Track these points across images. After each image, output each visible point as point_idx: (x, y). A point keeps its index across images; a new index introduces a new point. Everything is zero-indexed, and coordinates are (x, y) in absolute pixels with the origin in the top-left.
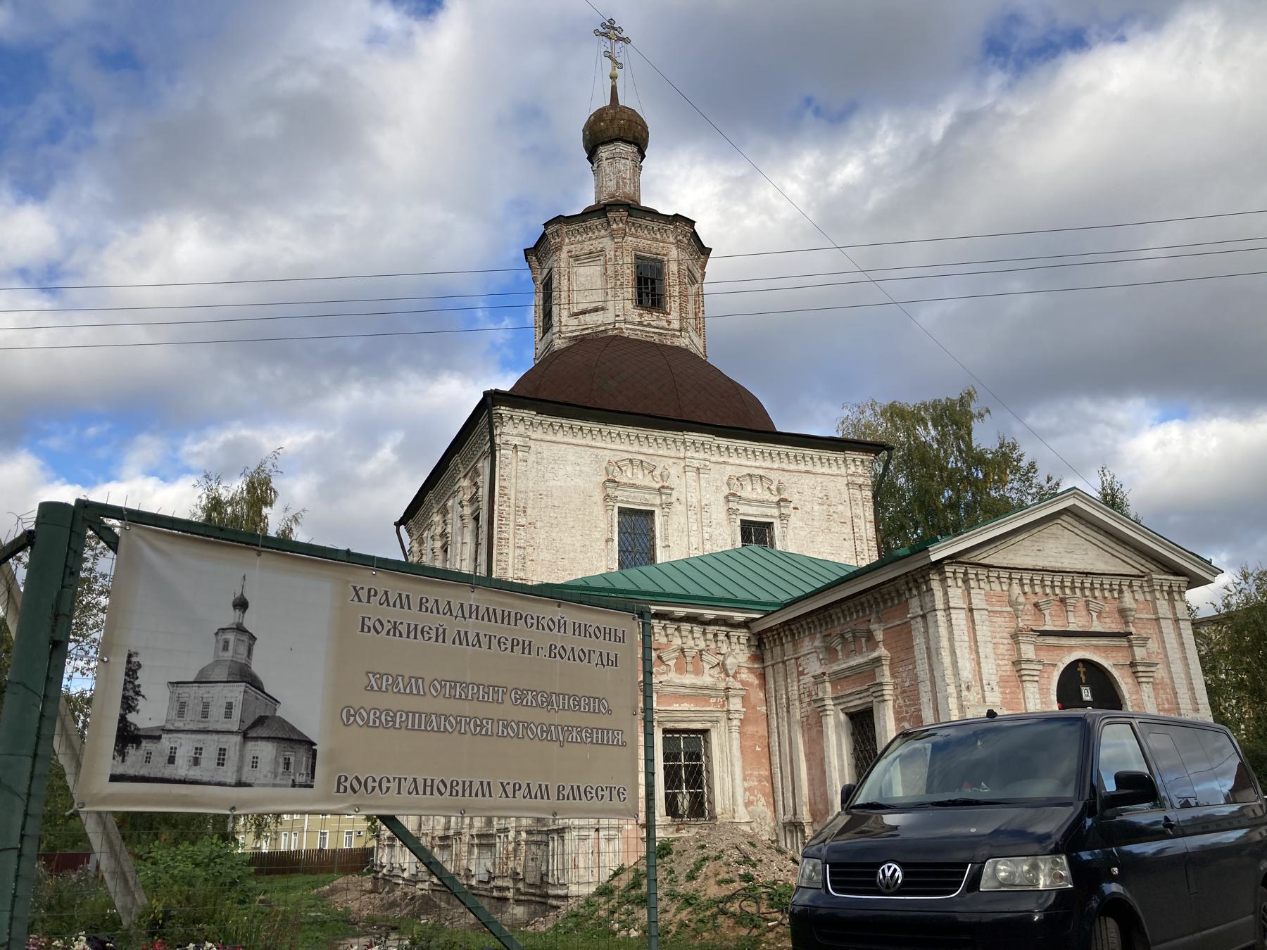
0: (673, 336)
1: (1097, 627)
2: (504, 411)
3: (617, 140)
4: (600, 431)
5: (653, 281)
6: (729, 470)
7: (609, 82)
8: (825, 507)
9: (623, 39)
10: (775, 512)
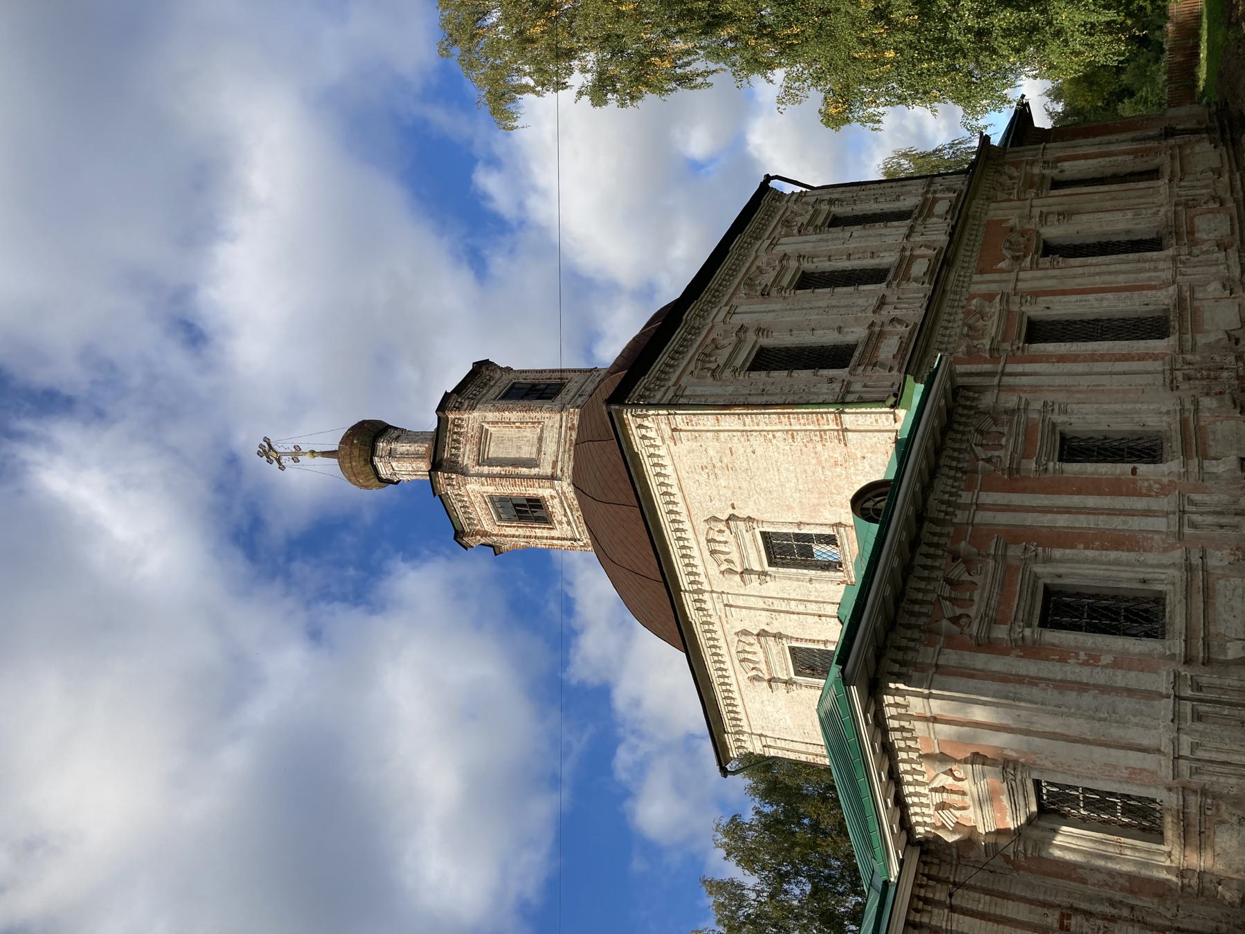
5: (515, 505)
7: (319, 459)
9: (269, 445)
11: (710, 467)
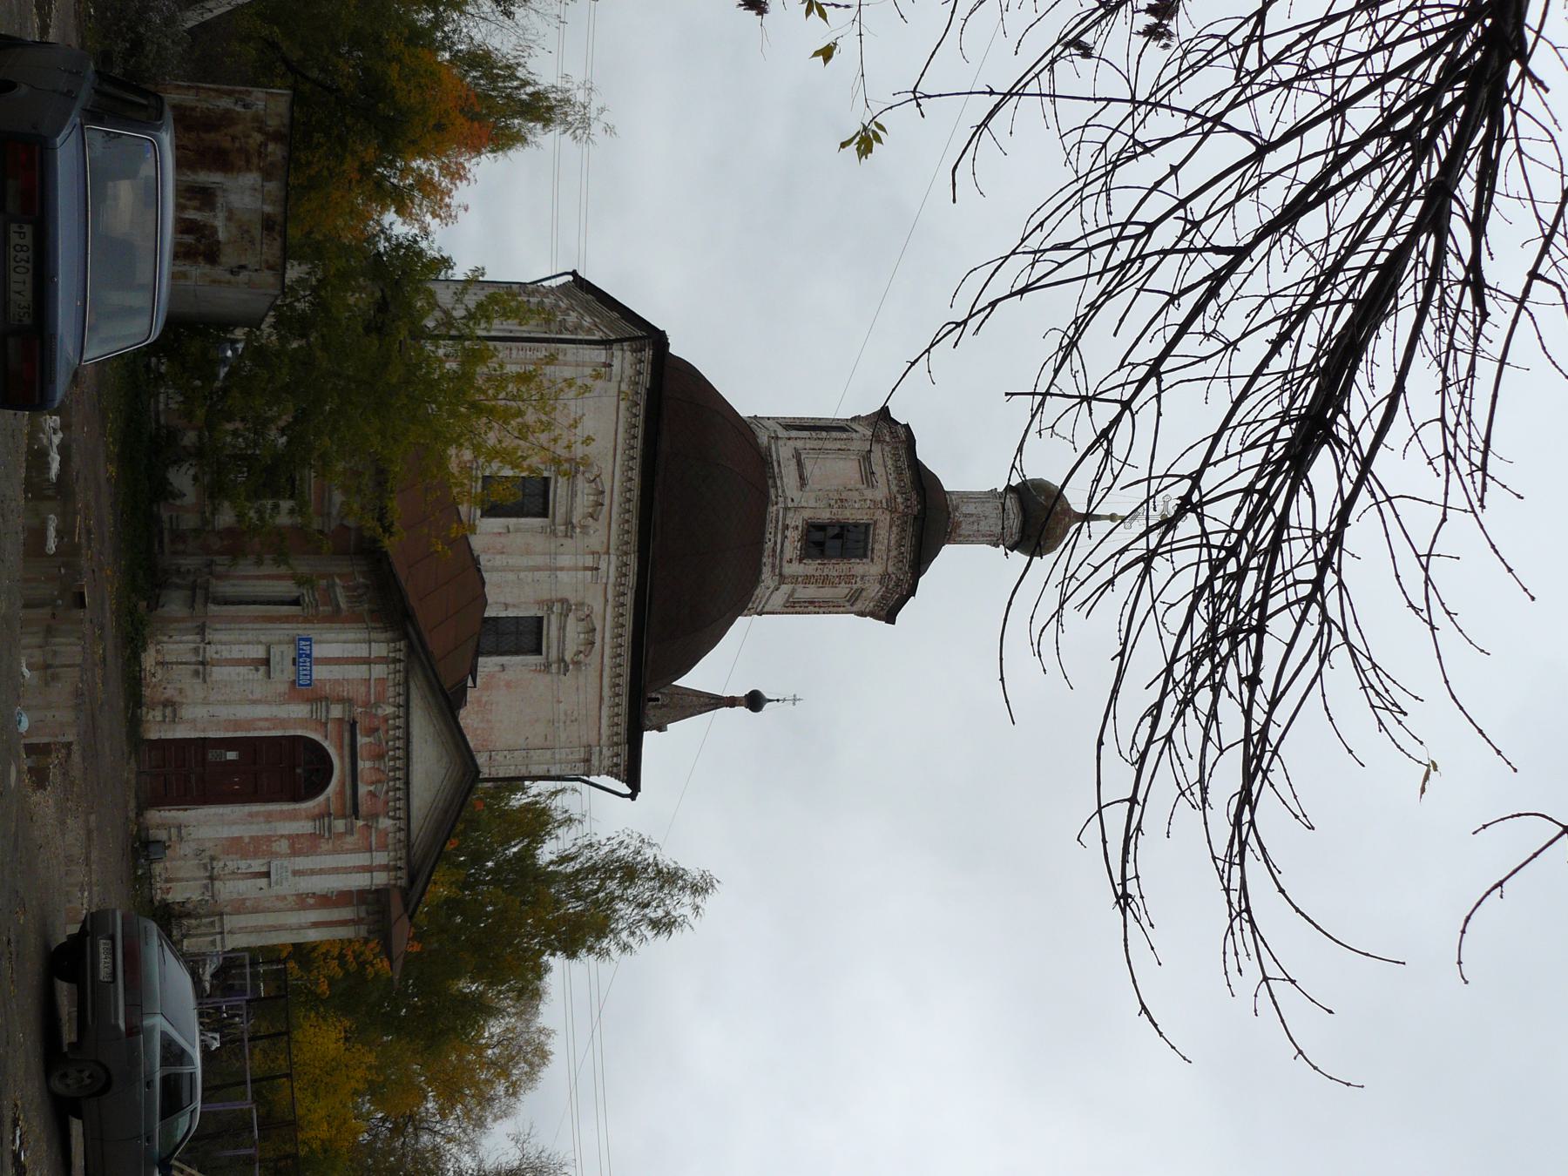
0: (773, 566)
1: (363, 789)
2: (648, 354)
3: (1024, 515)
4: (633, 458)
6: (598, 607)
8: (562, 717)
10: (554, 655)
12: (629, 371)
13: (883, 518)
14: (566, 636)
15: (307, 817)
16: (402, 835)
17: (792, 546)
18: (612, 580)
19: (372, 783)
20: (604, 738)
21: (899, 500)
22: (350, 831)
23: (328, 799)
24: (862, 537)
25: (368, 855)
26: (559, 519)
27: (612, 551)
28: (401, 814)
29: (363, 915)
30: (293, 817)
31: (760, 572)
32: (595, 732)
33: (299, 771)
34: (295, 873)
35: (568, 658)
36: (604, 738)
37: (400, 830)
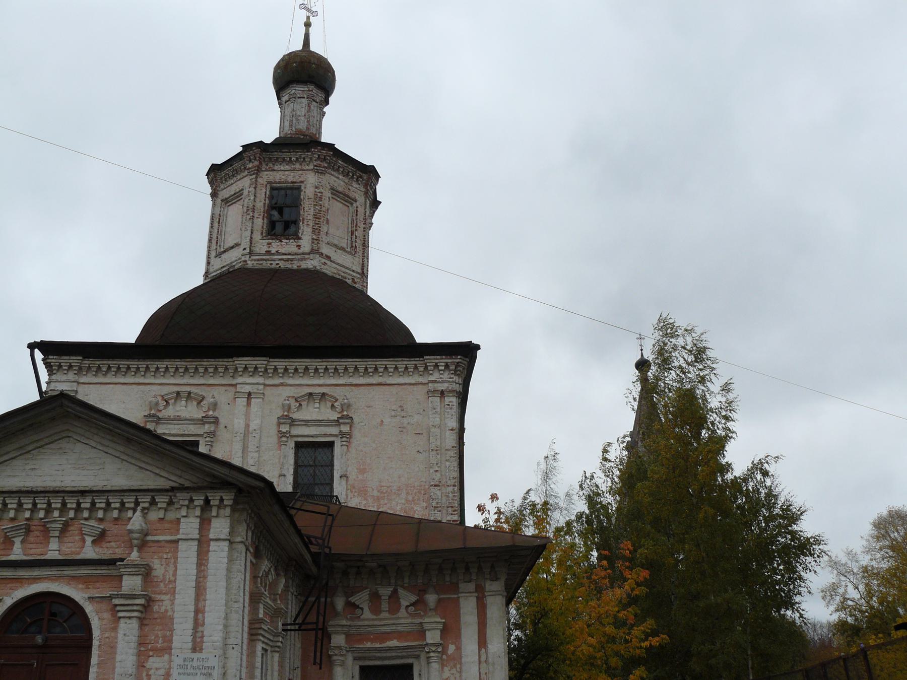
0: (302, 260)
1: (90, 552)
10: (334, 430)
11: (403, 414)
12: (71, 376)
13: (266, 176)
14: (315, 421)
15: (115, 629)
16: (162, 500)
17: (287, 247)
18: (261, 380)
19: (84, 541)
20: (421, 380)
21: (250, 165)
22: (146, 573)
23: (91, 599)
24: (283, 192)
25: (182, 546)
26: (201, 432)
27: (234, 382)
28: (129, 501)
29: (472, 586)
30: (111, 648)
31: (307, 270)
32: (415, 388)
33: (39, 639)
34: (197, 647)
35: (334, 416)
36: (421, 380)
37: (153, 502)
